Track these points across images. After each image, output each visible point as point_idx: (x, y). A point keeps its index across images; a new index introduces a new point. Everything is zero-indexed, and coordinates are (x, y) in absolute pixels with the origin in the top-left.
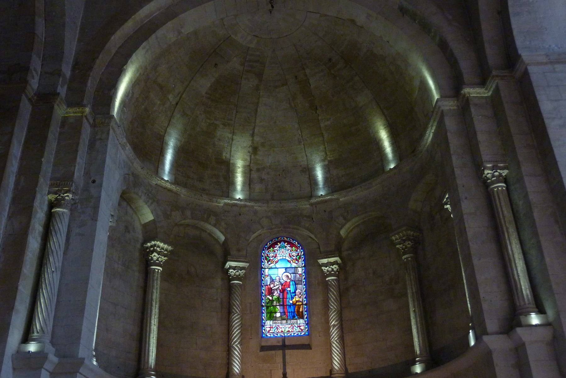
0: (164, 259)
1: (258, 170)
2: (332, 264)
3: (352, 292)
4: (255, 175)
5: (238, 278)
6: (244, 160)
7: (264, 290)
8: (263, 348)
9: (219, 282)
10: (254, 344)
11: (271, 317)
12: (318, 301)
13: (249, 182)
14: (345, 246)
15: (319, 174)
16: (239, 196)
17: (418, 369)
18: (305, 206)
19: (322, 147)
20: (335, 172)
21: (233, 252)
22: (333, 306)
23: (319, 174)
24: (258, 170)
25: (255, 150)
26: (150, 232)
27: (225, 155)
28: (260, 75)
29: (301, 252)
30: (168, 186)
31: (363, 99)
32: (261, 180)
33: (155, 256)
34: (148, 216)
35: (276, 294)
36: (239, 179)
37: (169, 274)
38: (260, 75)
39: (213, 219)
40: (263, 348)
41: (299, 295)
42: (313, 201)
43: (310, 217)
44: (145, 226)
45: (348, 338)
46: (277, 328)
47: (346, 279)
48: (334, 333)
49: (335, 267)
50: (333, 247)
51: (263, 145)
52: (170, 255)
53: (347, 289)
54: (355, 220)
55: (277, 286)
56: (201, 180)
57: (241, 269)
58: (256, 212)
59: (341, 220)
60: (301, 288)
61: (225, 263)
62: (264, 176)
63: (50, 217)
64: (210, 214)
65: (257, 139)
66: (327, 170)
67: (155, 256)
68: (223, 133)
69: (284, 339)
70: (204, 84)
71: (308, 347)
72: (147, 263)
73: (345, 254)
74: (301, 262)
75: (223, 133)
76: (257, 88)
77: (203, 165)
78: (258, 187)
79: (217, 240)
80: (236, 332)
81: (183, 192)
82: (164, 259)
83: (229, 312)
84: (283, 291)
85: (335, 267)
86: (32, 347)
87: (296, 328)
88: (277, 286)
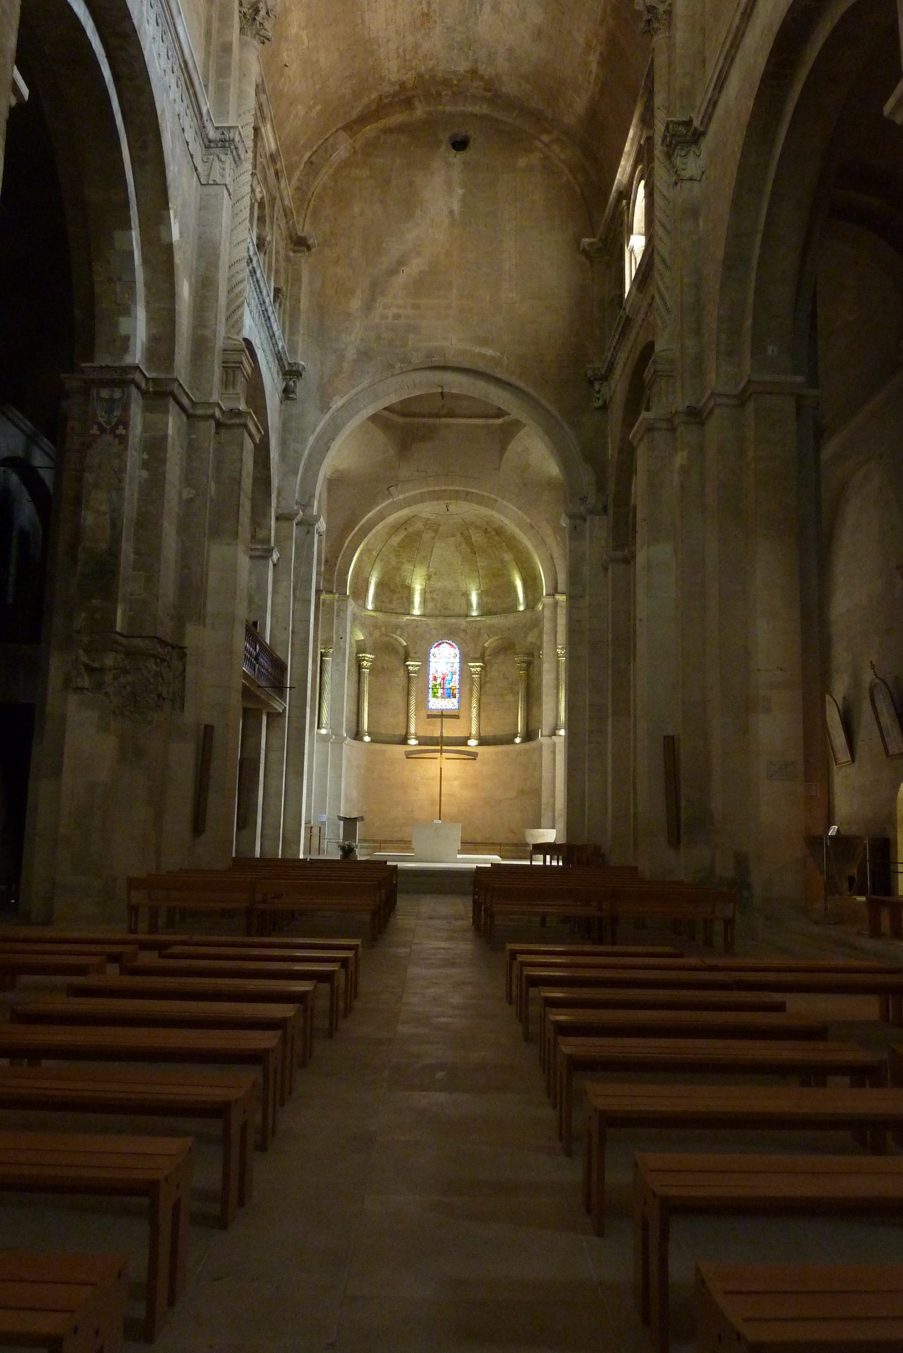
0: (369, 664)
1: (431, 592)
2: (477, 667)
3: (488, 685)
4: (428, 596)
5: (415, 672)
6: (422, 585)
7: (431, 677)
8: (429, 716)
9: (401, 673)
10: (423, 714)
11: (435, 696)
12: (466, 688)
13: (424, 602)
14: (488, 652)
15: (474, 598)
16: (417, 611)
17: (518, 740)
18: (462, 622)
19: (477, 580)
20: (485, 599)
21: (412, 654)
22: (475, 694)
23: (474, 598)
24: (431, 592)
25: (429, 577)
26: (361, 648)
27: (408, 582)
28: (436, 531)
29: (457, 651)
30: (372, 613)
31: (508, 557)
32: (433, 599)
33: (365, 663)
34: (360, 636)
35: (439, 681)
36: (417, 599)
37: (372, 669)
38: (436, 531)
39: (399, 632)
40: (429, 716)
41: (455, 682)
42: (469, 619)
43: (465, 631)
44: (358, 641)
45: (482, 714)
46: (436, 704)
47: (486, 675)
48: (474, 712)
49: (479, 669)
50: (478, 655)
51: (435, 574)
52: (373, 661)
53: (486, 683)
54: (497, 637)
55: (439, 675)
56: (391, 602)
57: (417, 666)
58: (427, 625)
59: (486, 637)
60: (456, 677)
61: (406, 661)
62: (435, 597)
63: (321, 660)
64: (398, 627)
65: (431, 570)
66: (480, 596)
67: (365, 663)
68: (407, 567)
69: (442, 711)
70: (396, 540)
71: (456, 717)
72: (360, 667)
73: (486, 658)
74: (457, 660)
75: (407, 567)
76: (434, 538)
77: (394, 592)
78: (430, 605)
79: (400, 643)
80: (412, 708)
81: (380, 615)
82: (369, 664)
83: (408, 694)
84: (443, 679)
85: (479, 669)
86: (323, 731)
87: (451, 704)
88: (439, 675)
